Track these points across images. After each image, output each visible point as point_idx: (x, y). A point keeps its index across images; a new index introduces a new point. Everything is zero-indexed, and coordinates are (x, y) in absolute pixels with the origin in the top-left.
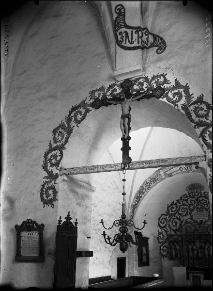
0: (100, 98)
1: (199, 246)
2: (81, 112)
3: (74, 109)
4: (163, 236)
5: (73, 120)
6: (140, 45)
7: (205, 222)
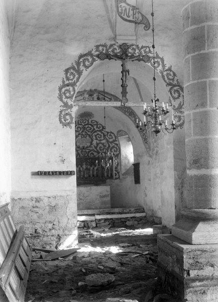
0: (104, 52)
1: (85, 168)
2: (88, 60)
3: (81, 56)
5: (82, 64)
6: (134, 20)
7: (87, 147)
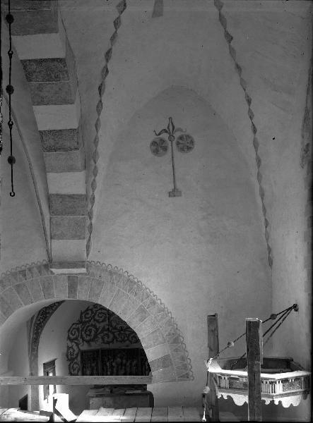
4: (74, 351)
